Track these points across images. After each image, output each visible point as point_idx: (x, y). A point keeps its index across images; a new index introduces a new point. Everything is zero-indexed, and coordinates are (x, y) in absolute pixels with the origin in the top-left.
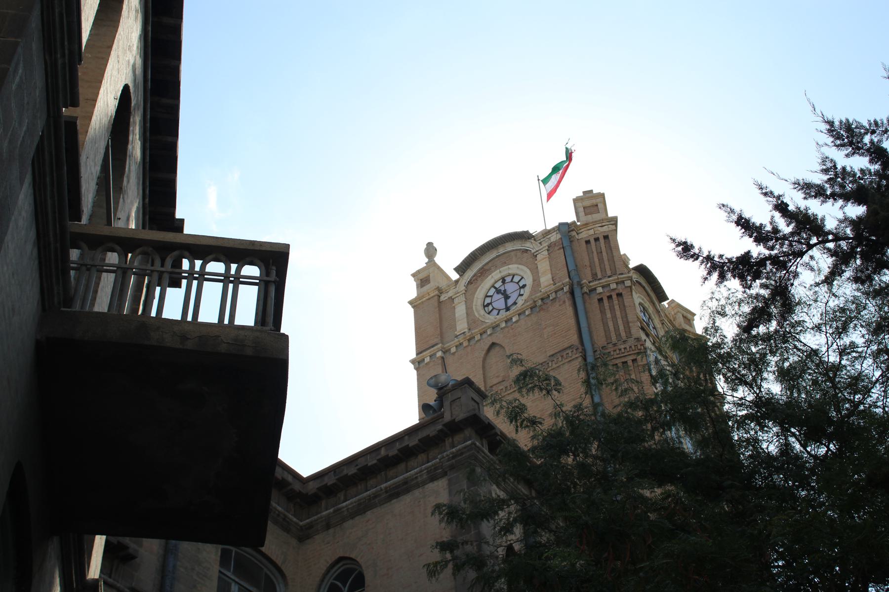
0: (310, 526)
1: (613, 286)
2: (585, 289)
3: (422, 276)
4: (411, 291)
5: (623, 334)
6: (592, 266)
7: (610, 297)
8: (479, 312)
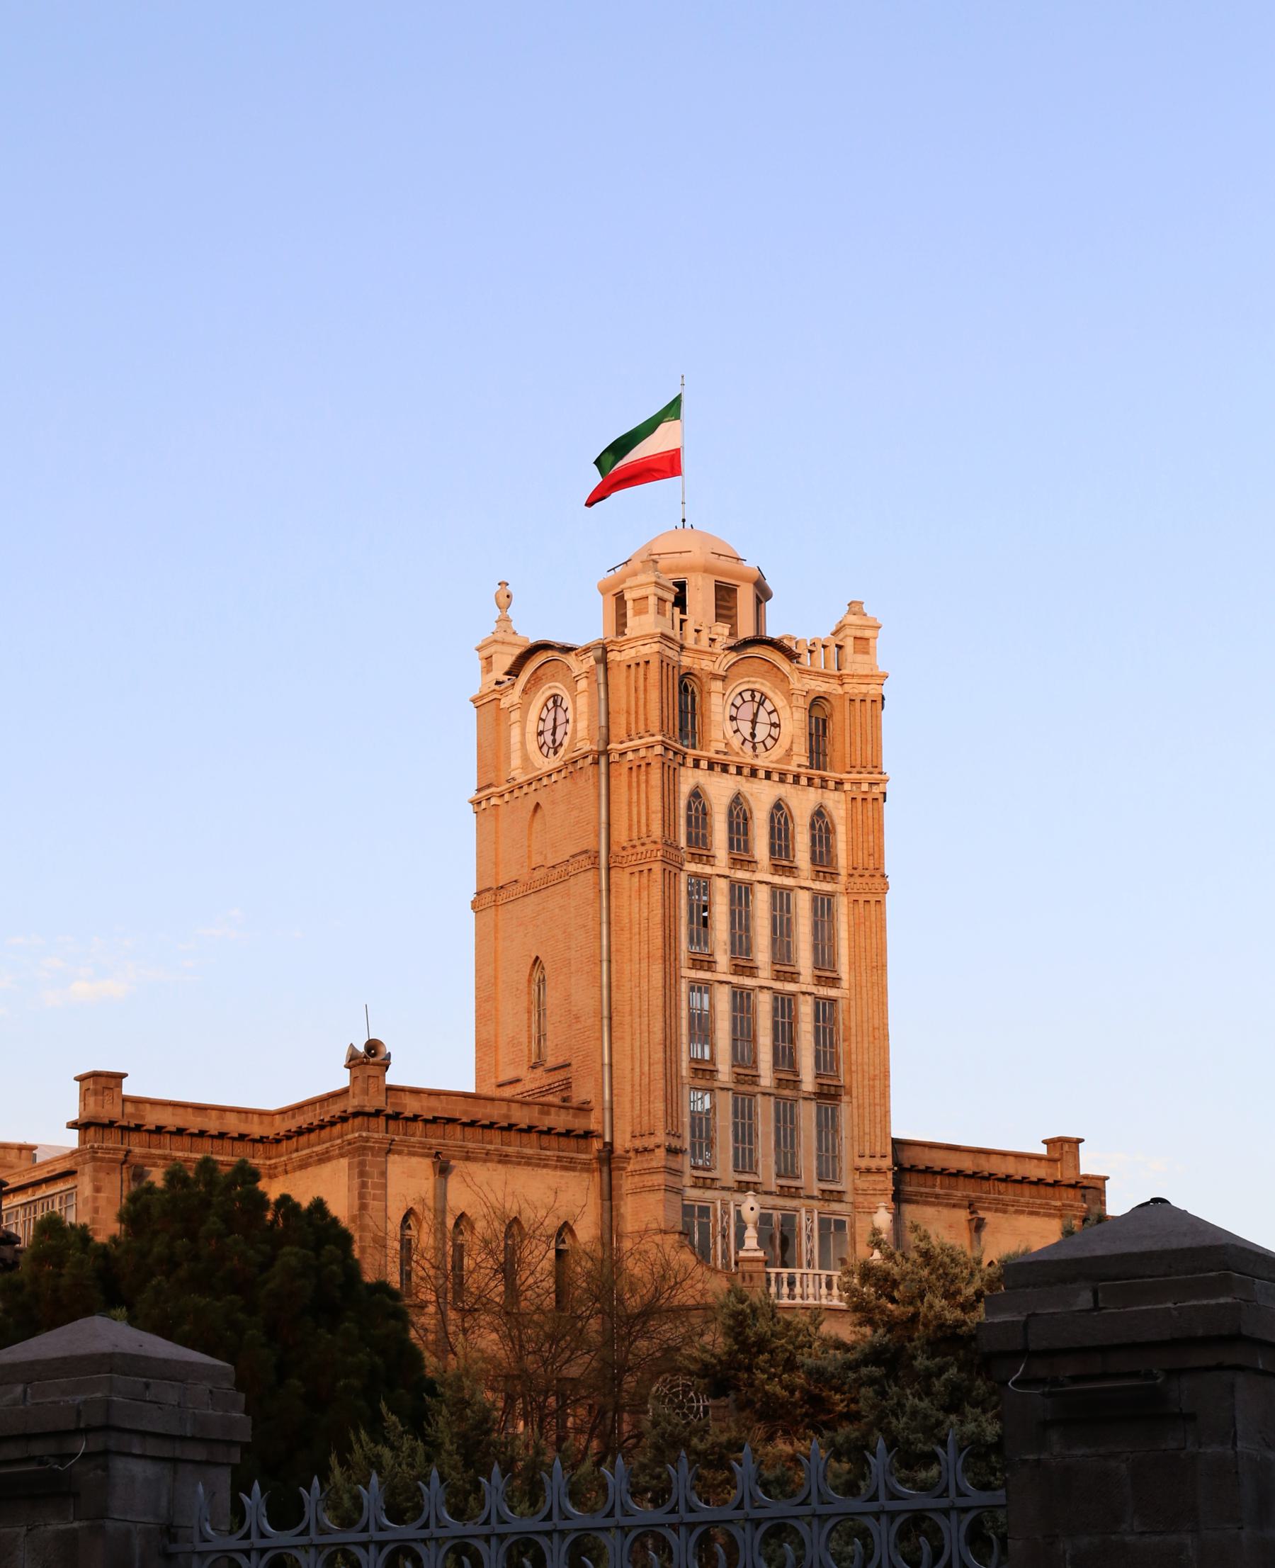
0: (275, 1167)
1: (642, 753)
2: (614, 757)
3: (486, 653)
4: (474, 681)
5: (644, 829)
6: (628, 712)
7: (639, 766)
8: (532, 746)
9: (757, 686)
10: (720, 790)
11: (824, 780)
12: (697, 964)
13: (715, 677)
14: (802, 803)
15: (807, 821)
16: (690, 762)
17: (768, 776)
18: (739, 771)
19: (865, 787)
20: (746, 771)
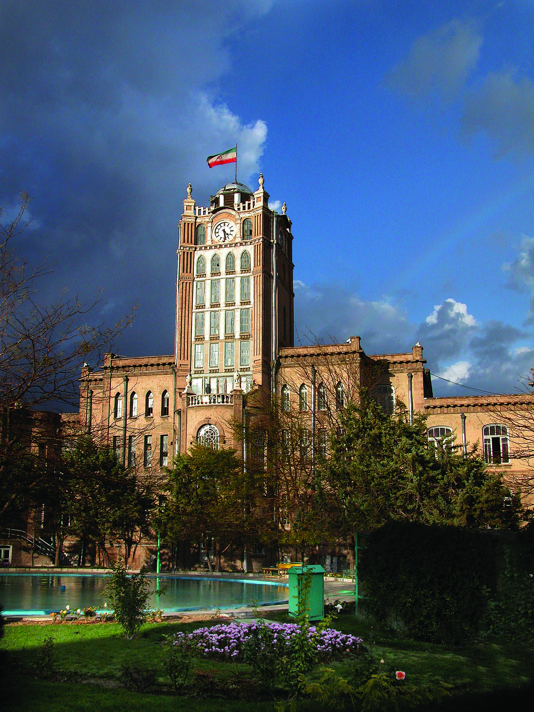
9: (225, 221)
10: (208, 255)
11: (246, 242)
12: (197, 307)
13: (208, 222)
14: (238, 252)
15: (240, 257)
16: (198, 249)
17: (226, 246)
18: (216, 247)
19: (257, 241)
20: (218, 247)
